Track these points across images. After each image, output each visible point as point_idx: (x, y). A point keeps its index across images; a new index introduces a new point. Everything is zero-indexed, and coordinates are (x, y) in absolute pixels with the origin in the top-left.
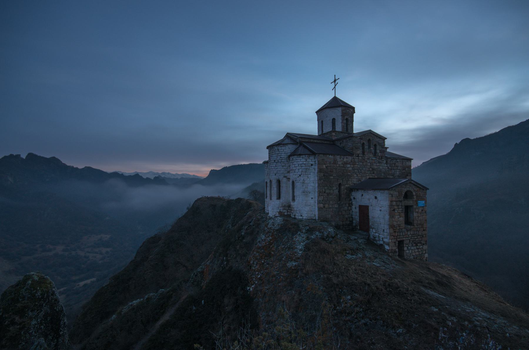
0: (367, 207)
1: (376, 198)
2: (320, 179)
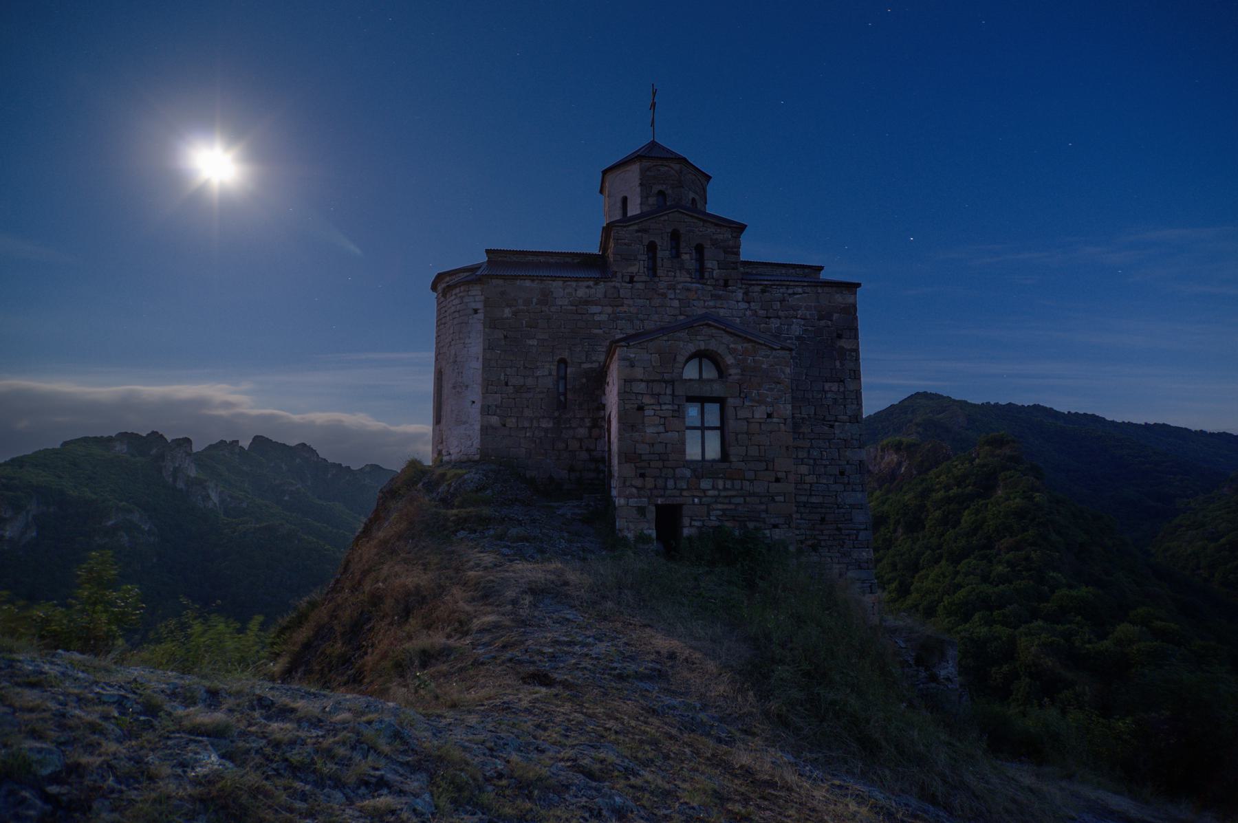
2: (489, 347)
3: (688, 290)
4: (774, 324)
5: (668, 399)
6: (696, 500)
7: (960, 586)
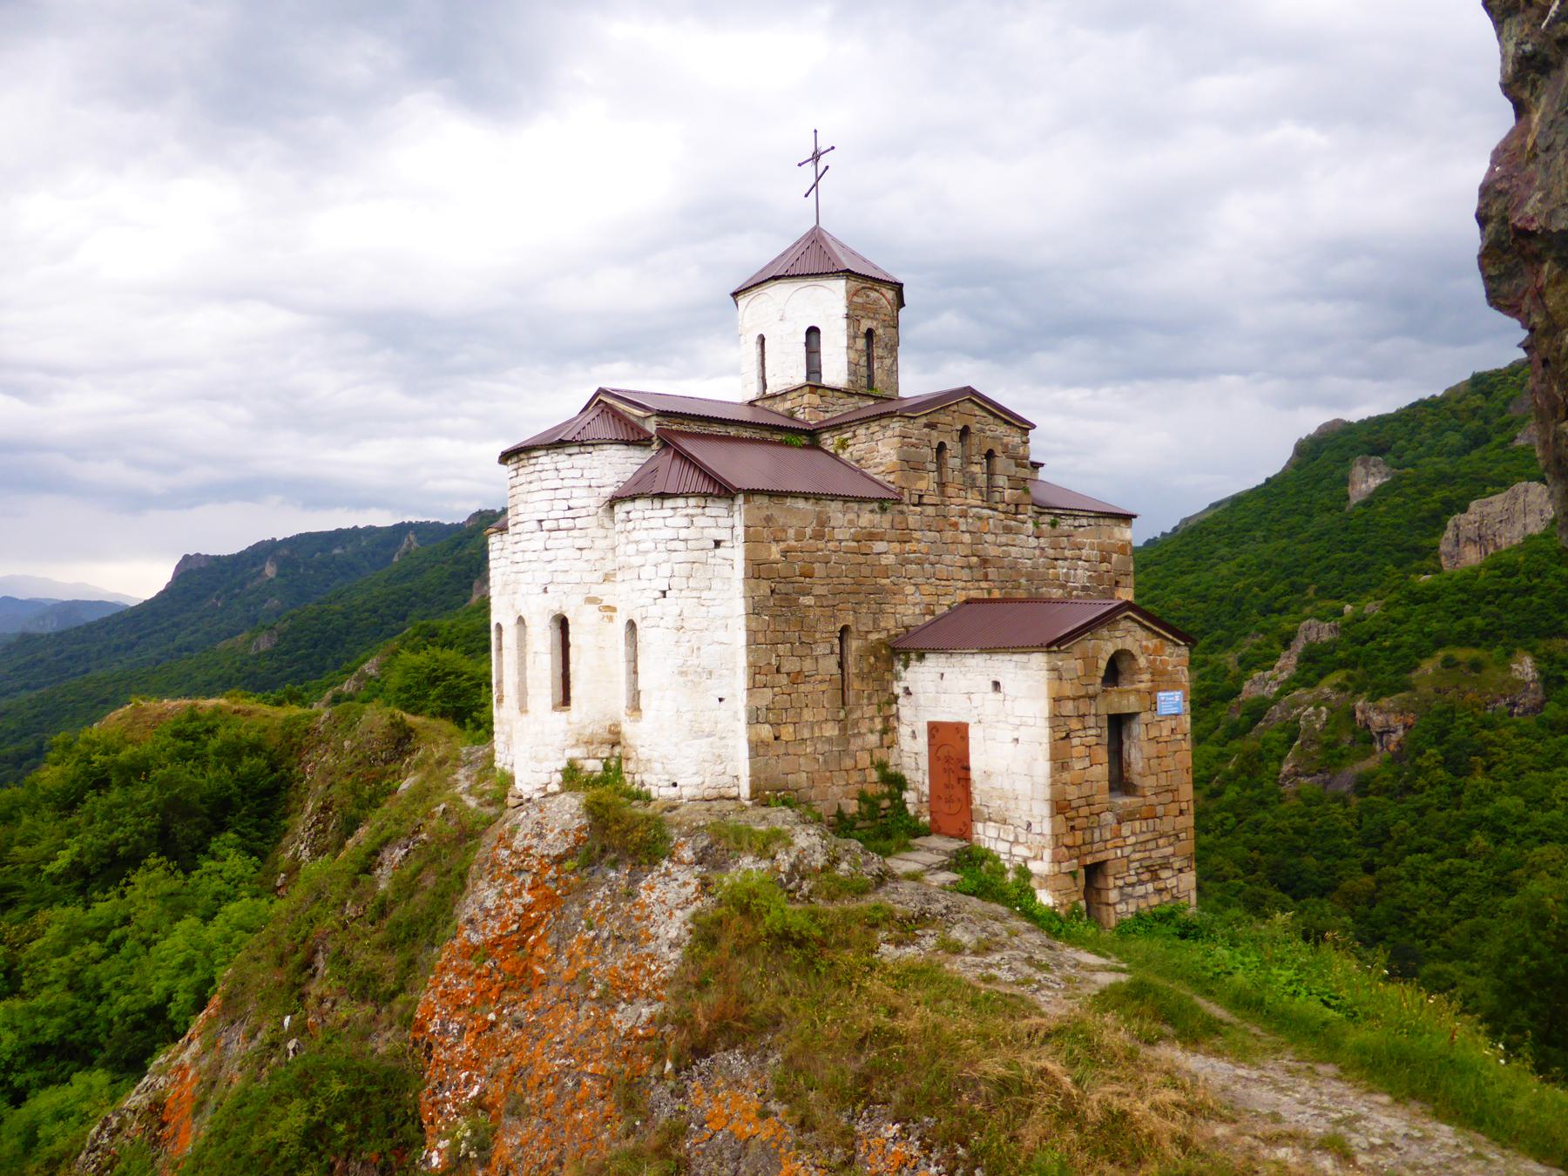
0: (959, 732)
1: (996, 685)
2: (754, 610)
3: (980, 518)
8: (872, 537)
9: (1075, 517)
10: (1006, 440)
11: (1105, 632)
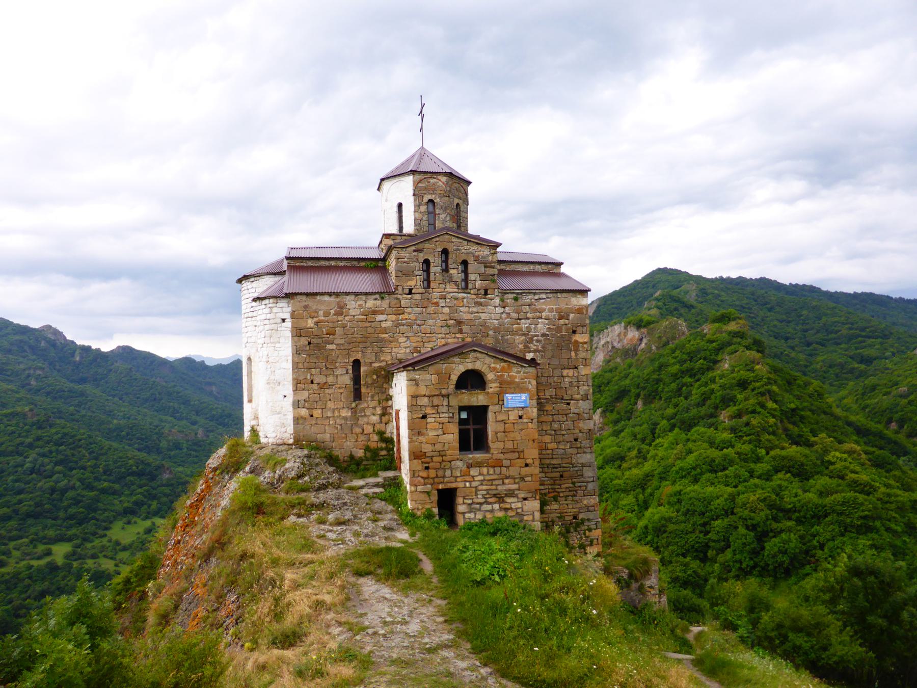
2: (297, 352)
3: (457, 299)
4: (524, 324)
5: (445, 409)
6: (468, 484)
7: (690, 452)
8: (375, 313)
9: (535, 294)
10: (477, 254)
11: (456, 359)
